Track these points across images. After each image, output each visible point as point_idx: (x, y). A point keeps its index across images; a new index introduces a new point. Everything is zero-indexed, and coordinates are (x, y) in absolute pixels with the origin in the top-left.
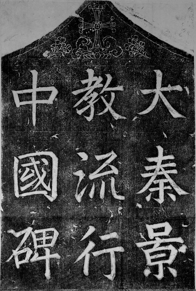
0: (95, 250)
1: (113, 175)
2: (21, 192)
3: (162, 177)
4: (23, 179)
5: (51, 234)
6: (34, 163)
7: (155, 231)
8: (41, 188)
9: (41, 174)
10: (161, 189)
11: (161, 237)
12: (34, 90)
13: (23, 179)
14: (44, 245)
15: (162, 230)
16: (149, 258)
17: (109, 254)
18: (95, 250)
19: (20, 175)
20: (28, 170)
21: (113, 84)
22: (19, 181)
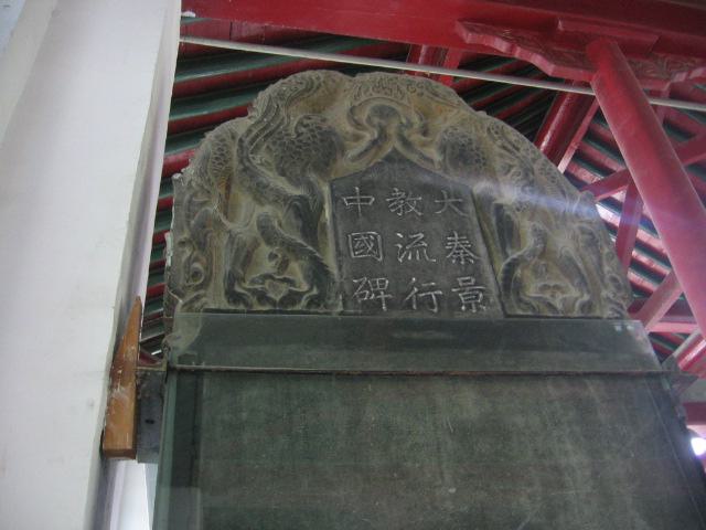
0: (419, 292)
3: (461, 249)
7: (464, 281)
10: (462, 255)
15: (469, 281)
18: (419, 292)
19: (353, 245)
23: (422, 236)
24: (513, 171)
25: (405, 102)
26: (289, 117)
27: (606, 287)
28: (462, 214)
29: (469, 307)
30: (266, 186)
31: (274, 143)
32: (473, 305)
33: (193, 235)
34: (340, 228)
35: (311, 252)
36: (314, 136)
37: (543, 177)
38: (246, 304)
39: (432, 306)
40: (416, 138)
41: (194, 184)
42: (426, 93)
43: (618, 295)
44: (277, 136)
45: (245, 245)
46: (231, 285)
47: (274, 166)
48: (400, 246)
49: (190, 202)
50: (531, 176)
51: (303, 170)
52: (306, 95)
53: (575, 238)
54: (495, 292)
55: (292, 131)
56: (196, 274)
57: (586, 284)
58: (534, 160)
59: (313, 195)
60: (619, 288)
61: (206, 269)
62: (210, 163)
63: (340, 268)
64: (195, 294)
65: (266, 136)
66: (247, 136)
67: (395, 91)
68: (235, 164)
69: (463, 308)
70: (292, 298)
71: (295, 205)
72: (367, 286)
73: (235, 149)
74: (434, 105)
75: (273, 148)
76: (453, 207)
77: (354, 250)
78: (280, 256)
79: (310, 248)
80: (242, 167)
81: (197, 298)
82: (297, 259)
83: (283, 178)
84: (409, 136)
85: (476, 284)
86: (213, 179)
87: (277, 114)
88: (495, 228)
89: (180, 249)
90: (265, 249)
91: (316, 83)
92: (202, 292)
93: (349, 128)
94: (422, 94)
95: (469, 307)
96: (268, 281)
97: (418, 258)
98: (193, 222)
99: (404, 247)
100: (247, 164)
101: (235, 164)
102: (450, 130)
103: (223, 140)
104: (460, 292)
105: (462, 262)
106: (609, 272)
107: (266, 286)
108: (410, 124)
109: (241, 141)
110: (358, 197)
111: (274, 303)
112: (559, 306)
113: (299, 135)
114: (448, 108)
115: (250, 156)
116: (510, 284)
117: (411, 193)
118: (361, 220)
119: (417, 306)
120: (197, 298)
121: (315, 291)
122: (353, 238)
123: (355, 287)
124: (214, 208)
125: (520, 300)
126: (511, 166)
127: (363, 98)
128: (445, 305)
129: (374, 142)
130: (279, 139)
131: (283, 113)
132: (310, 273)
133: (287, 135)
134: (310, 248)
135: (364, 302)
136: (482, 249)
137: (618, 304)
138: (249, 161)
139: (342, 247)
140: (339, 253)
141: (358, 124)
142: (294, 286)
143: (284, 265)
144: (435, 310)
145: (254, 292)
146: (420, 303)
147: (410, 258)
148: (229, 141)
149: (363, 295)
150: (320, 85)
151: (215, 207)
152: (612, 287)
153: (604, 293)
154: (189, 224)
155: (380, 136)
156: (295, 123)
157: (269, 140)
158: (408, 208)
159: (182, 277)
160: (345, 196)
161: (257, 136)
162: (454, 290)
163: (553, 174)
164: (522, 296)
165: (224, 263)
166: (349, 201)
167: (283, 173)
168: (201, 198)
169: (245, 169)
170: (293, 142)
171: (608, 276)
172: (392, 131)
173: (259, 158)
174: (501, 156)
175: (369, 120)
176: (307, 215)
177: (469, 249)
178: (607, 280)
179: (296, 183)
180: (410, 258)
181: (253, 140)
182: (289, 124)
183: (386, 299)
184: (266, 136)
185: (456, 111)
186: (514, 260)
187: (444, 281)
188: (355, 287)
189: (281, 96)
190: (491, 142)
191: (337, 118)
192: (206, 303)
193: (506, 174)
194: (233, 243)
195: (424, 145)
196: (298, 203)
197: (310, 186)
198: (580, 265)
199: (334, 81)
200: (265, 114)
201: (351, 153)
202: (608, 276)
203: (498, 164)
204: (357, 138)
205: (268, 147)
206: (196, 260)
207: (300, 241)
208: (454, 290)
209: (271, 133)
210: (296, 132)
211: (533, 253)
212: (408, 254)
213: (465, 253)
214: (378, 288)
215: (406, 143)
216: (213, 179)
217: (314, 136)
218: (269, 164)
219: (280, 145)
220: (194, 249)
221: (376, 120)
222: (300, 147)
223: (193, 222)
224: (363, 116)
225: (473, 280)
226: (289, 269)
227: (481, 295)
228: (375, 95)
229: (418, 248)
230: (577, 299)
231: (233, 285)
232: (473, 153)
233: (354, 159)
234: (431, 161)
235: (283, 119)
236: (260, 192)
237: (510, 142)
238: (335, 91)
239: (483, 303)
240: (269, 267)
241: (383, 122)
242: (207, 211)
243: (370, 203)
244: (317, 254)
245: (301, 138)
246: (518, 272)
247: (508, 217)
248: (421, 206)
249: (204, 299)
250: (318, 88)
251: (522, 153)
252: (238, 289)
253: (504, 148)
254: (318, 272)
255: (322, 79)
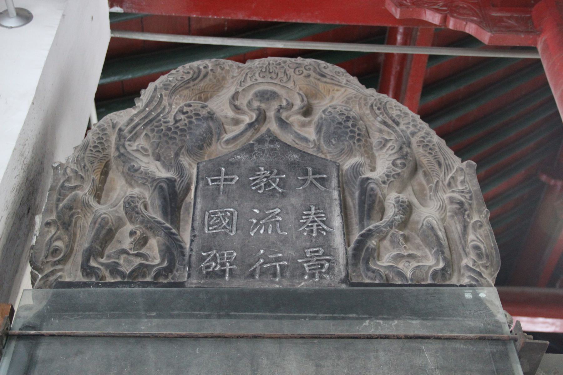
0: (264, 263)
1: (278, 221)
2: (209, 230)
3: (316, 222)
4: (211, 223)
5: (232, 254)
6: (220, 214)
7: (311, 252)
8: (225, 228)
9: (225, 220)
10: (315, 228)
11: (317, 256)
12: (222, 178)
13: (211, 223)
14: (225, 260)
15: (317, 252)
16: (307, 269)
17: (276, 266)
18: (264, 263)
19: (209, 221)
20: (215, 218)
21: (278, 174)
22: (208, 224)
23: (278, 211)
24: (390, 144)
25: (290, 85)
26: (170, 105)
27: (467, 255)
28: (323, 188)
29: (312, 276)
30: (136, 170)
31: (152, 130)
32: (317, 275)
33: (59, 217)
34: (199, 207)
35: (167, 228)
36: (191, 122)
37: (421, 150)
38: (97, 277)
39: (275, 275)
40: (295, 119)
41: (68, 171)
42: (313, 74)
43: (480, 262)
44: (155, 124)
45: (107, 223)
46: (86, 260)
47: (150, 152)
48: (255, 221)
49: (62, 186)
50: (406, 149)
51: (177, 155)
52: (192, 83)
53: (442, 208)
54: (342, 261)
55: (171, 119)
56: (56, 251)
57: (443, 253)
58: (413, 134)
59: (181, 176)
60: (480, 256)
61: (67, 246)
62: (88, 152)
63: (192, 241)
64: (52, 269)
65: (146, 125)
66: (127, 126)
67: (281, 75)
68: (113, 152)
69: (306, 277)
70: (142, 270)
71: (161, 187)
72: (214, 259)
73: (113, 138)
74: (321, 86)
75: (151, 135)
76: (314, 182)
77: (209, 226)
78: (138, 233)
79: (168, 225)
80: (117, 154)
81: (53, 273)
82: (155, 235)
83: (158, 163)
84: (287, 118)
85: (324, 254)
86: (88, 165)
87: (160, 102)
88: (357, 201)
89: (47, 229)
90: (129, 227)
91: (203, 71)
92: (59, 267)
93: (231, 113)
94: (309, 76)
95: (312, 276)
96: (123, 256)
97: (270, 232)
98: (61, 205)
99: (258, 221)
100: (122, 151)
101: (113, 152)
102: (329, 110)
103: (103, 130)
104: (306, 262)
105: (314, 235)
106: (473, 241)
107: (121, 262)
108: (290, 105)
109: (120, 130)
110: (222, 178)
111: (123, 275)
112: (409, 275)
113: (176, 121)
114: (336, 88)
115: (127, 143)
116: (361, 253)
117: (276, 171)
118: (222, 197)
119: (260, 275)
120: (53, 273)
121: (165, 264)
122: (210, 215)
123: (203, 259)
124: (84, 192)
125: (368, 269)
126: (387, 141)
127: (249, 83)
128: (288, 274)
129: (251, 125)
130: (157, 127)
131: (165, 102)
132: (164, 247)
133: (165, 122)
134: (168, 225)
135: (208, 273)
136: (337, 222)
137: (474, 271)
138: (125, 148)
139: (197, 224)
140: (193, 229)
141: (237, 109)
142: (147, 259)
143: (144, 241)
144: (277, 279)
145: (107, 266)
146: (263, 273)
147: (262, 232)
148: (109, 131)
149: (208, 267)
150: (207, 73)
151: (86, 191)
152: (473, 256)
153: (465, 261)
154: (57, 208)
155: (257, 120)
156: (176, 110)
157: (149, 127)
158: (270, 185)
159: (43, 255)
160: (209, 177)
161: (137, 125)
162: (299, 261)
163: (431, 146)
164: (372, 266)
165: (84, 242)
166: (213, 181)
167: (158, 159)
168: (73, 184)
169: (121, 155)
170: (169, 129)
171: (470, 245)
172: (271, 114)
173: (141, 142)
174: (381, 131)
175: (249, 103)
176: (172, 199)
177: (323, 222)
178: (469, 249)
179: (167, 167)
180: (262, 232)
181: (134, 128)
182: (169, 112)
183: (230, 269)
184: (146, 125)
185: (343, 90)
186: (370, 230)
187: (292, 253)
188: (203, 259)
189: (166, 86)
190: (372, 119)
191: (220, 105)
192: (61, 277)
193: (381, 149)
194: (95, 223)
195: (303, 125)
196: (165, 186)
197: (180, 170)
198: (441, 234)
199: (223, 69)
200: (147, 105)
201: (226, 137)
202: (470, 245)
203: (375, 139)
204: (236, 122)
205: (146, 134)
206: (59, 239)
207: (159, 219)
208: (299, 261)
209: (151, 121)
210: (175, 118)
211: (390, 225)
212: (261, 228)
213: (317, 226)
214: (225, 260)
215: (283, 123)
216: (88, 165)
217: (191, 122)
218: (146, 150)
219: (157, 132)
220: (58, 229)
221: (256, 104)
222: (176, 133)
223: (61, 205)
224: (243, 102)
225: (322, 251)
226: (148, 245)
227: (327, 265)
228: (260, 80)
229: (272, 223)
230: (430, 267)
231: (88, 260)
232: (348, 130)
233: (228, 142)
234: (306, 140)
235: (164, 109)
236: (132, 174)
237: (391, 118)
238: (224, 78)
239: (327, 272)
240: (127, 243)
241: (263, 106)
242: (76, 195)
243: (233, 183)
244: (174, 231)
245: (178, 124)
246: (372, 243)
247: (372, 189)
248: (283, 184)
249: (59, 274)
250: (205, 76)
251: (402, 127)
252: (93, 263)
253: (385, 123)
254: (173, 249)
255: (210, 68)
